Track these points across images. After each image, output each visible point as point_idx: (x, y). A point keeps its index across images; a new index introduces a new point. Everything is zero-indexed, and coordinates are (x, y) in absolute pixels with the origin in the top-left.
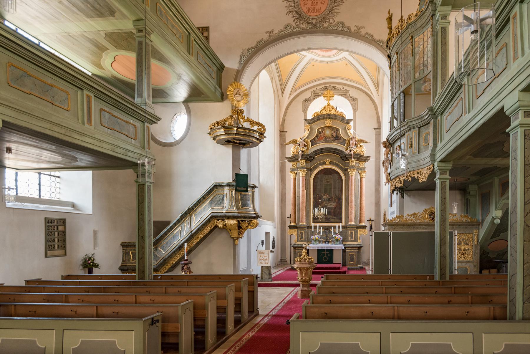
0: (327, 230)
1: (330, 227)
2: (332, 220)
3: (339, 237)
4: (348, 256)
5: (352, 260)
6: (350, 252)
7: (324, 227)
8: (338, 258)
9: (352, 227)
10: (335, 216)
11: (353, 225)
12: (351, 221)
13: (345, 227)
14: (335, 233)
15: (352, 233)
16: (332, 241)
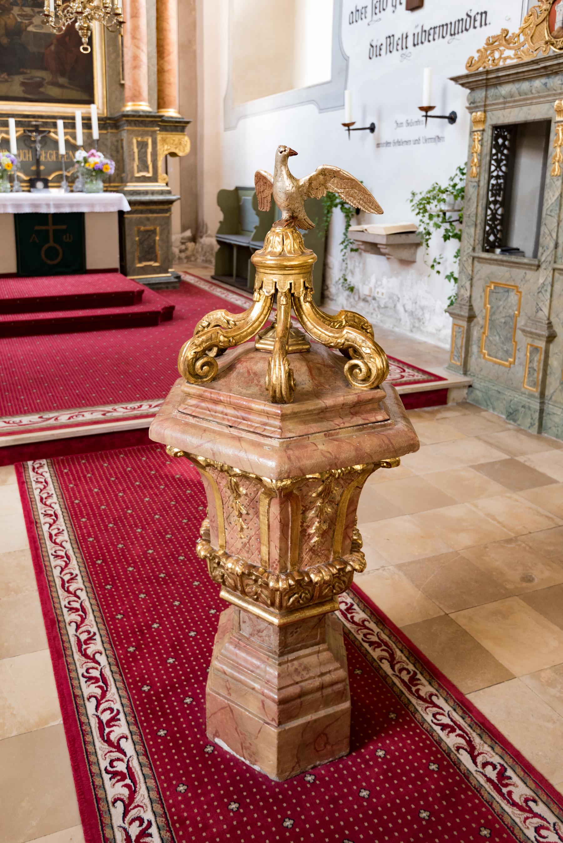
0: (35, 132)
1: (50, 121)
2: (54, 92)
3: (98, 159)
4: (133, 238)
5: (148, 253)
6: (141, 222)
7: (23, 121)
8: (101, 249)
9: (140, 120)
10: (63, 75)
11: (147, 116)
12: (136, 97)
13: (111, 123)
14: (72, 147)
15: (142, 146)
16: (59, 179)
